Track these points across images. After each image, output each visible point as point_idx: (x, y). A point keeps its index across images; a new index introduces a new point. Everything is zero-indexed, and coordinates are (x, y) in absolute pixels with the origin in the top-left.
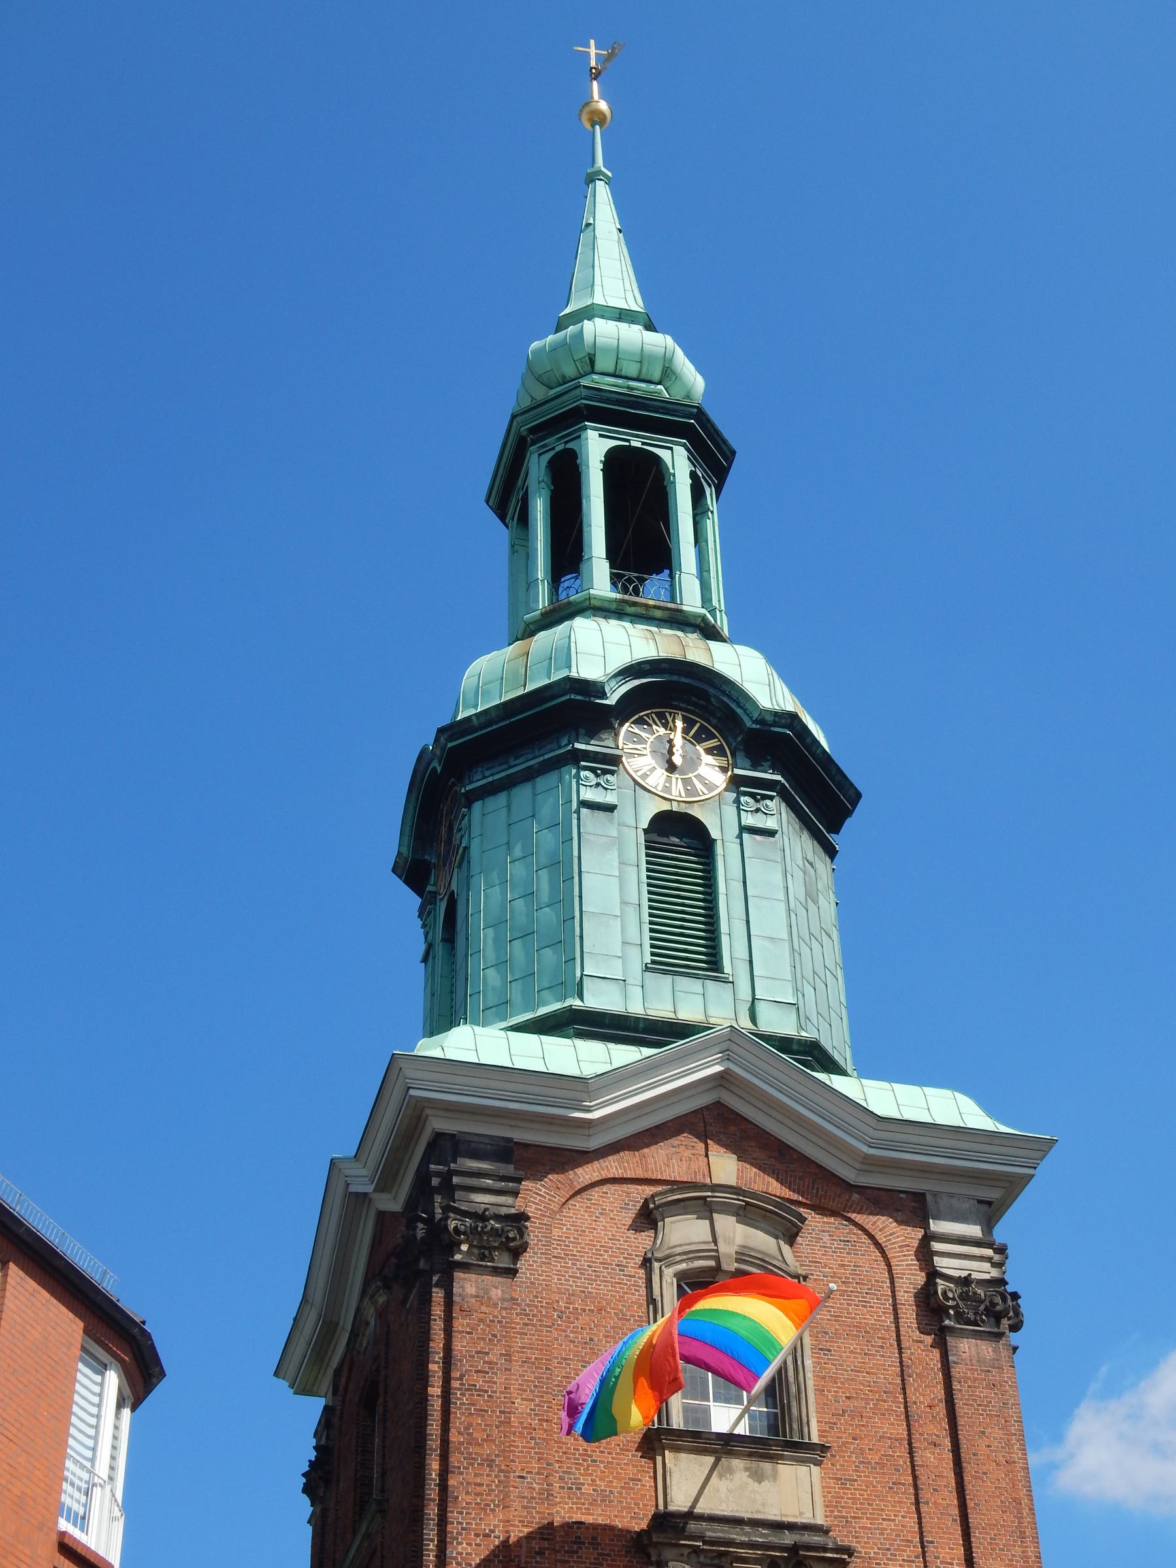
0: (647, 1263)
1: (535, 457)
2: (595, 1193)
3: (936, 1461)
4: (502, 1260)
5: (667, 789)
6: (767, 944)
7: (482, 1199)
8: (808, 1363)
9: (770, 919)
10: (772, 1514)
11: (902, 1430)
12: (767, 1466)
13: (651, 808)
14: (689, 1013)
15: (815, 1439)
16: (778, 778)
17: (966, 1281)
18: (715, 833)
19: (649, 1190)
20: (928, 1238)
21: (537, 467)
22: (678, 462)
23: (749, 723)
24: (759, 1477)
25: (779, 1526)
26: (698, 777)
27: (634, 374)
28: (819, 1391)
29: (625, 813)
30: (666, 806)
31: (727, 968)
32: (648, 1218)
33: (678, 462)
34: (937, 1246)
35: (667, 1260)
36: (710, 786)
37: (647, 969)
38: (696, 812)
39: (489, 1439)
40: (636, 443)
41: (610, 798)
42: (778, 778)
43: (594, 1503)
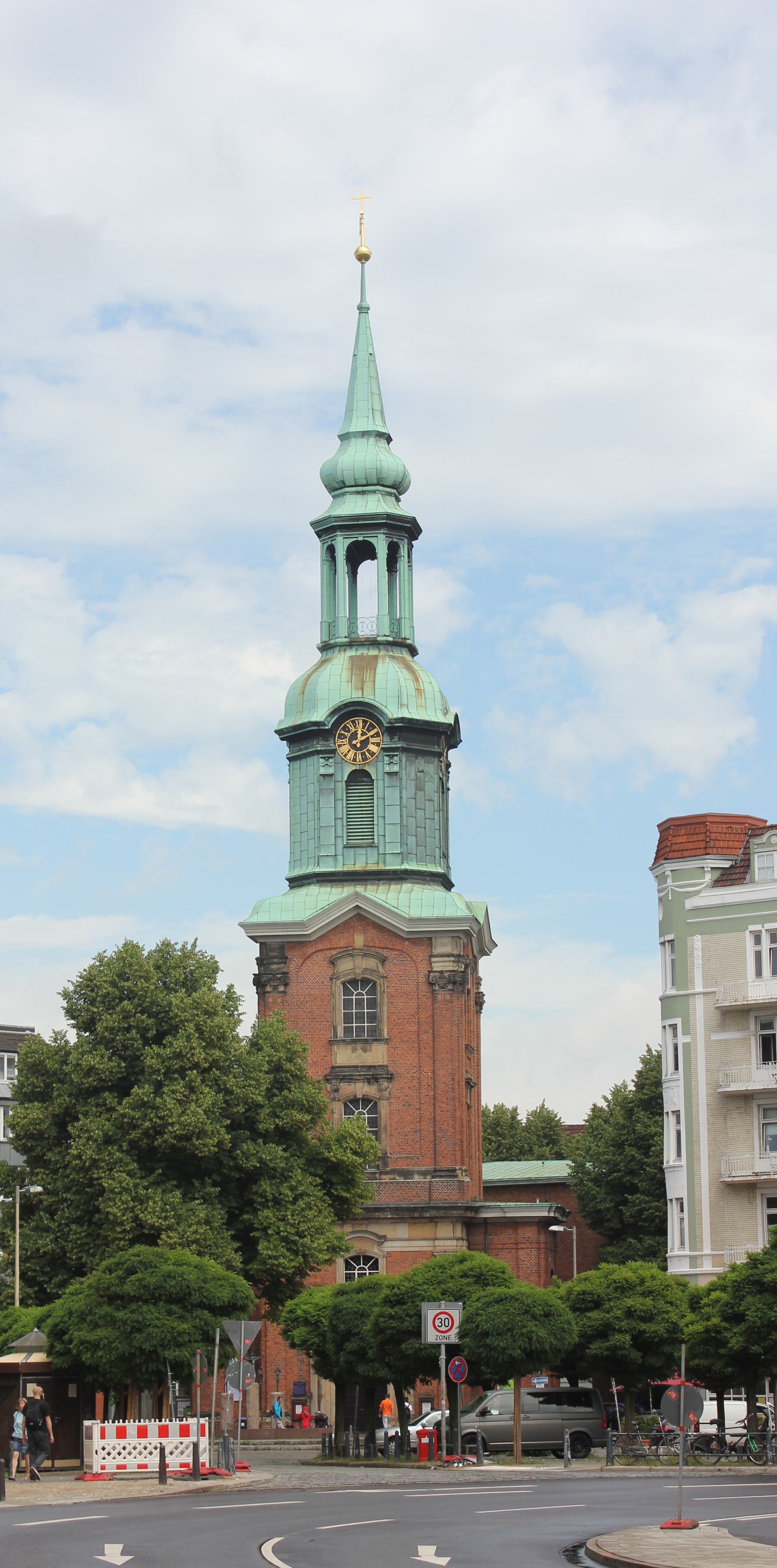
0: (331, 979)
3: (426, 1038)
4: (281, 988)
5: (355, 760)
6: (392, 826)
7: (274, 967)
10: (369, 1063)
11: (416, 1028)
12: (368, 1047)
13: (348, 769)
15: (386, 1037)
17: (441, 972)
18: (374, 777)
19: (334, 952)
23: (385, 724)
24: (365, 1050)
25: (370, 1067)
26: (369, 751)
27: (364, 482)
30: (354, 768)
31: (376, 841)
33: (381, 544)
34: (433, 959)
35: (338, 978)
36: (372, 754)
38: (367, 768)
40: (361, 539)
41: (331, 771)
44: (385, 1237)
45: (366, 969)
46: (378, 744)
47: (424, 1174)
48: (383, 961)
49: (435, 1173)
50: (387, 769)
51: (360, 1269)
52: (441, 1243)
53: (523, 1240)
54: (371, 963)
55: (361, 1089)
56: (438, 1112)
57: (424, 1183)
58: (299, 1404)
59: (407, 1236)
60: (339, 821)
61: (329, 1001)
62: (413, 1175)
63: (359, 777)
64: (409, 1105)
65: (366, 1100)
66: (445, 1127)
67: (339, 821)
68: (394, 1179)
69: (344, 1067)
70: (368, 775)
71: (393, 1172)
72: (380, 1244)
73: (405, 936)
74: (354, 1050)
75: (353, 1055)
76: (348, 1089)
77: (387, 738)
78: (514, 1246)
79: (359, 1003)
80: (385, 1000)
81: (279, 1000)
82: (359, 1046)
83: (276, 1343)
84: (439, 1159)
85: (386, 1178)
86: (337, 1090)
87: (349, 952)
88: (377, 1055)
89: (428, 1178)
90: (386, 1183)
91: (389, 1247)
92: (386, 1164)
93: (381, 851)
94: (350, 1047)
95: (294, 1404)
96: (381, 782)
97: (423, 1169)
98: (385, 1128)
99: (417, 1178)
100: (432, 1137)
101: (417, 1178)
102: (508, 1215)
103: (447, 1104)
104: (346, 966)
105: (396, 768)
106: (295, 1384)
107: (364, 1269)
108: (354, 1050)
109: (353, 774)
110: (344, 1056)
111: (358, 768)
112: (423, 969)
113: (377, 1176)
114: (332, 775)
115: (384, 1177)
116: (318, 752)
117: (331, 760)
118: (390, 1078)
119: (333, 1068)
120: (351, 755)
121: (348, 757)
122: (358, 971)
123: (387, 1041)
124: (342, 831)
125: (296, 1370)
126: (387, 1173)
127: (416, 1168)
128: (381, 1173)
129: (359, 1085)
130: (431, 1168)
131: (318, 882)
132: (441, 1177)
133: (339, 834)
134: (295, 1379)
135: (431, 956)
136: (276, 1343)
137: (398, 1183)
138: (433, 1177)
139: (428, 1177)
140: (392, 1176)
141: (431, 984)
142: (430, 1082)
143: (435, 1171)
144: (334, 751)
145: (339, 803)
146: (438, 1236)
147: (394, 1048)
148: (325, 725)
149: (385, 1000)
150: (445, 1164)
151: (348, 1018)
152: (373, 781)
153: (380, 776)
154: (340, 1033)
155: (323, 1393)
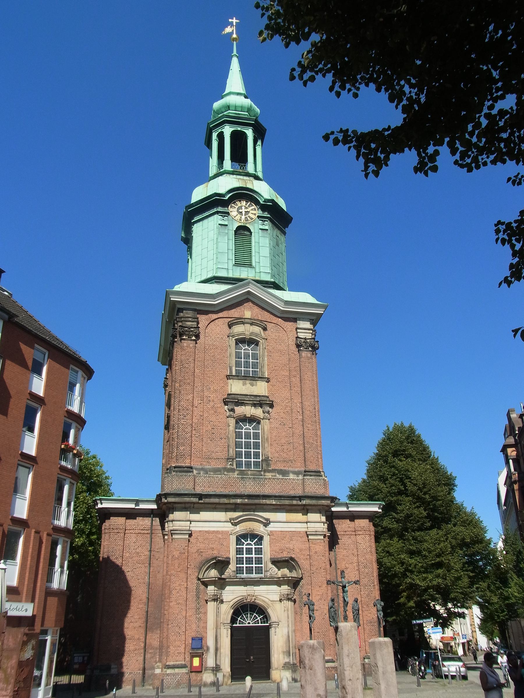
0: (228, 336)
1: (214, 133)
2: (216, 321)
3: (296, 380)
5: (240, 220)
7: (189, 324)
8: (266, 359)
9: (265, 251)
10: (255, 393)
11: (287, 374)
12: (254, 382)
13: (236, 225)
14: (243, 276)
16: (269, 216)
17: (305, 339)
19: (230, 320)
20: (297, 329)
21: (215, 136)
22: (250, 133)
24: (252, 385)
25: (256, 396)
26: (249, 217)
28: (268, 365)
29: (230, 227)
30: (240, 224)
32: (230, 326)
34: (298, 330)
36: (252, 219)
37: (234, 265)
39: (189, 379)
41: (226, 223)
42: (269, 216)
43: (213, 392)
44: (267, 520)
45: (252, 334)
46: (255, 214)
47: (297, 473)
48: (265, 329)
49: (306, 473)
50: (261, 227)
51: (248, 544)
52: (312, 525)
53: (360, 529)
54: (257, 329)
55: (248, 411)
56: (306, 430)
57: (298, 480)
58: (196, 656)
59: (285, 520)
60: (230, 251)
61: (226, 350)
62: (289, 474)
63: (243, 231)
64: (284, 425)
65: (252, 420)
66: (311, 441)
67: (230, 251)
68: (275, 476)
69: (238, 395)
70: (248, 230)
71: (273, 471)
72: (266, 525)
73: (279, 315)
74: (244, 384)
75: (244, 387)
76: (240, 410)
77: (261, 212)
78: (354, 533)
79: (247, 356)
80: (266, 354)
81: (191, 345)
82: (248, 382)
83: (178, 604)
84: (308, 463)
85: (269, 475)
86: (233, 410)
87: (240, 321)
88: (260, 389)
89: (301, 477)
90: (270, 479)
91: (272, 527)
92: (268, 465)
93: (257, 271)
94: (241, 382)
95: (193, 656)
96: (257, 234)
97: (296, 470)
98: (267, 439)
99: (292, 476)
100: (302, 448)
101: (292, 476)
102: (350, 509)
103: (312, 425)
104: (238, 329)
105: (267, 227)
106: (193, 639)
107: (250, 544)
108: (244, 384)
109: (239, 228)
110: (237, 387)
111: (242, 224)
112: (292, 336)
113: (262, 473)
114: (227, 225)
115: (267, 474)
116: (217, 213)
117: (226, 217)
118: (271, 406)
119: (229, 395)
120: (238, 217)
121: (236, 218)
122: (247, 333)
123: (268, 380)
124: (232, 256)
125: (194, 626)
126: (269, 471)
127: (290, 469)
128: (265, 471)
129: (248, 408)
130: (303, 469)
131: (216, 282)
132: (311, 476)
133: (230, 257)
134: (194, 634)
135: (297, 329)
136: (178, 604)
137: (278, 479)
138: (304, 475)
139: (300, 476)
140: (274, 474)
141: (298, 346)
142: (299, 410)
143: (305, 472)
144: (228, 213)
145: (230, 242)
146: (309, 520)
147: (273, 386)
148: (224, 197)
149: (266, 354)
150: (312, 467)
151: (238, 364)
152: (251, 233)
153: (257, 230)
154: (234, 373)
155: (219, 646)
